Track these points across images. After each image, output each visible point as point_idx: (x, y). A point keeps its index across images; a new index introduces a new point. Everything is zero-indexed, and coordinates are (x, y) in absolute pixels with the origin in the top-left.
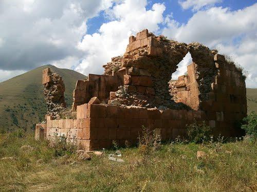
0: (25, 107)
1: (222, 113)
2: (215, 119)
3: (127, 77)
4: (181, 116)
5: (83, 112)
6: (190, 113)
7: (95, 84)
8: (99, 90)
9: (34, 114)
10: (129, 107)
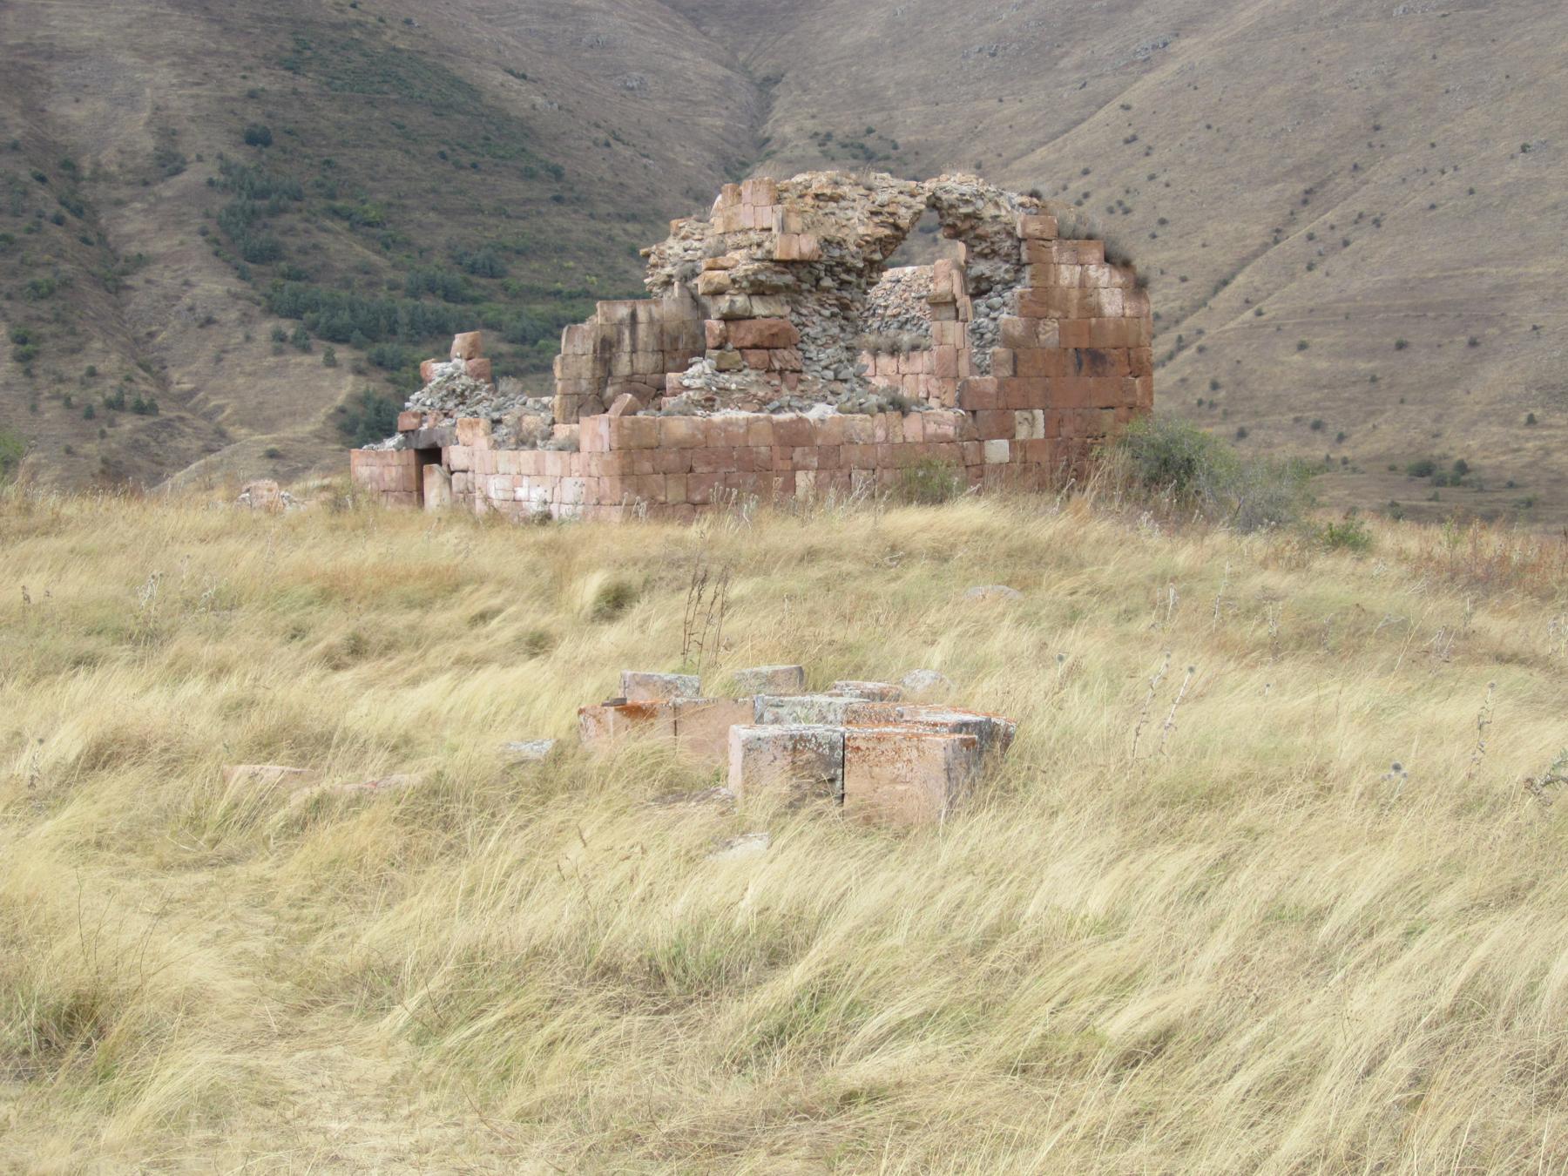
1: (1039, 414)
2: (1008, 432)
4: (880, 434)
7: (620, 333)
8: (634, 351)
10: (717, 417)
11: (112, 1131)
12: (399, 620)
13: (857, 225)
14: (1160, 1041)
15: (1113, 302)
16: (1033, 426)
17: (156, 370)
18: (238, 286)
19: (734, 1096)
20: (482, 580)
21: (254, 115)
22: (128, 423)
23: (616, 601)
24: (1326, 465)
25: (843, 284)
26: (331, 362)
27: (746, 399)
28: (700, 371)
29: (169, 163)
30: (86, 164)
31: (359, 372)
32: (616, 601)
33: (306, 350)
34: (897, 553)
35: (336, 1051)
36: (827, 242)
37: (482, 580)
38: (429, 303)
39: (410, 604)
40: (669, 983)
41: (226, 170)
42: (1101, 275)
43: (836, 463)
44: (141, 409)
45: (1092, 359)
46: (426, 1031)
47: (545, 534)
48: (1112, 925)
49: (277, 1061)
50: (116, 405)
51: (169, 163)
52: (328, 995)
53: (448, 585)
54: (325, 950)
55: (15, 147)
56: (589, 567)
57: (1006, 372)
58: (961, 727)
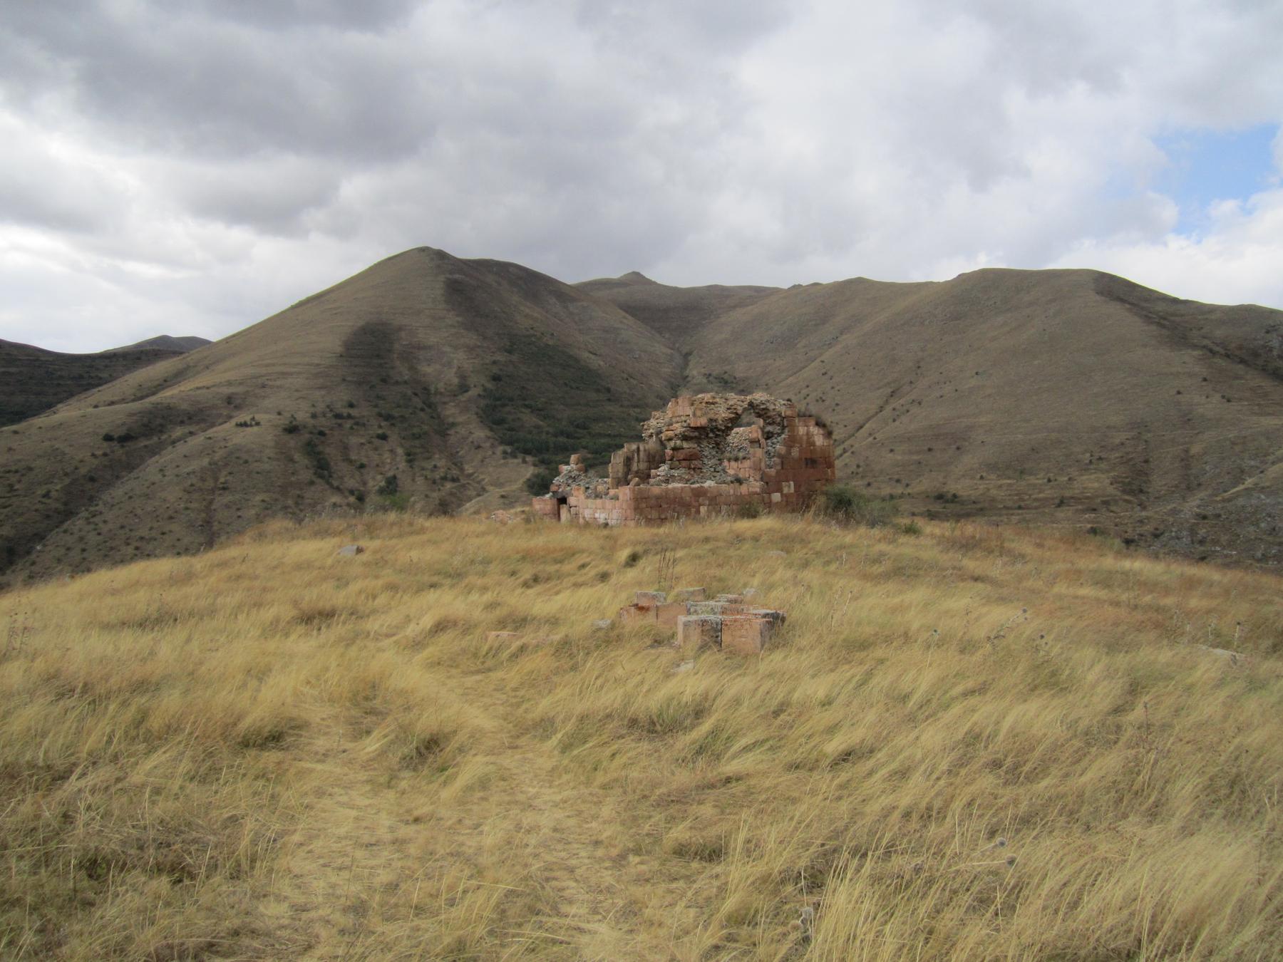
0: (349, 416)
2: (780, 490)
9: (383, 437)
10: (670, 486)
11: (446, 794)
12: (551, 568)
13: (722, 413)
14: (847, 756)
15: (819, 440)
16: (789, 488)
17: (459, 465)
18: (489, 434)
19: (684, 778)
20: (582, 551)
21: (495, 370)
22: (449, 485)
23: (634, 559)
24: (902, 496)
25: (717, 436)
26: (524, 462)
27: (681, 479)
28: (663, 469)
29: (464, 388)
30: (433, 390)
31: (535, 465)
32: (634, 559)
33: (515, 457)
34: (739, 538)
35: (530, 755)
36: (711, 420)
37: (582, 551)
38: (561, 439)
39: (556, 561)
40: (655, 727)
41: (485, 390)
42: (815, 430)
43: (715, 502)
44: (454, 480)
45: (811, 462)
46: (566, 747)
47: (606, 532)
48: (827, 703)
49: (509, 761)
50: (444, 479)
51: (464, 388)
52: (527, 730)
53: (571, 553)
54: (526, 711)
55: (406, 382)
56: (625, 546)
57: (779, 467)
58: (765, 616)
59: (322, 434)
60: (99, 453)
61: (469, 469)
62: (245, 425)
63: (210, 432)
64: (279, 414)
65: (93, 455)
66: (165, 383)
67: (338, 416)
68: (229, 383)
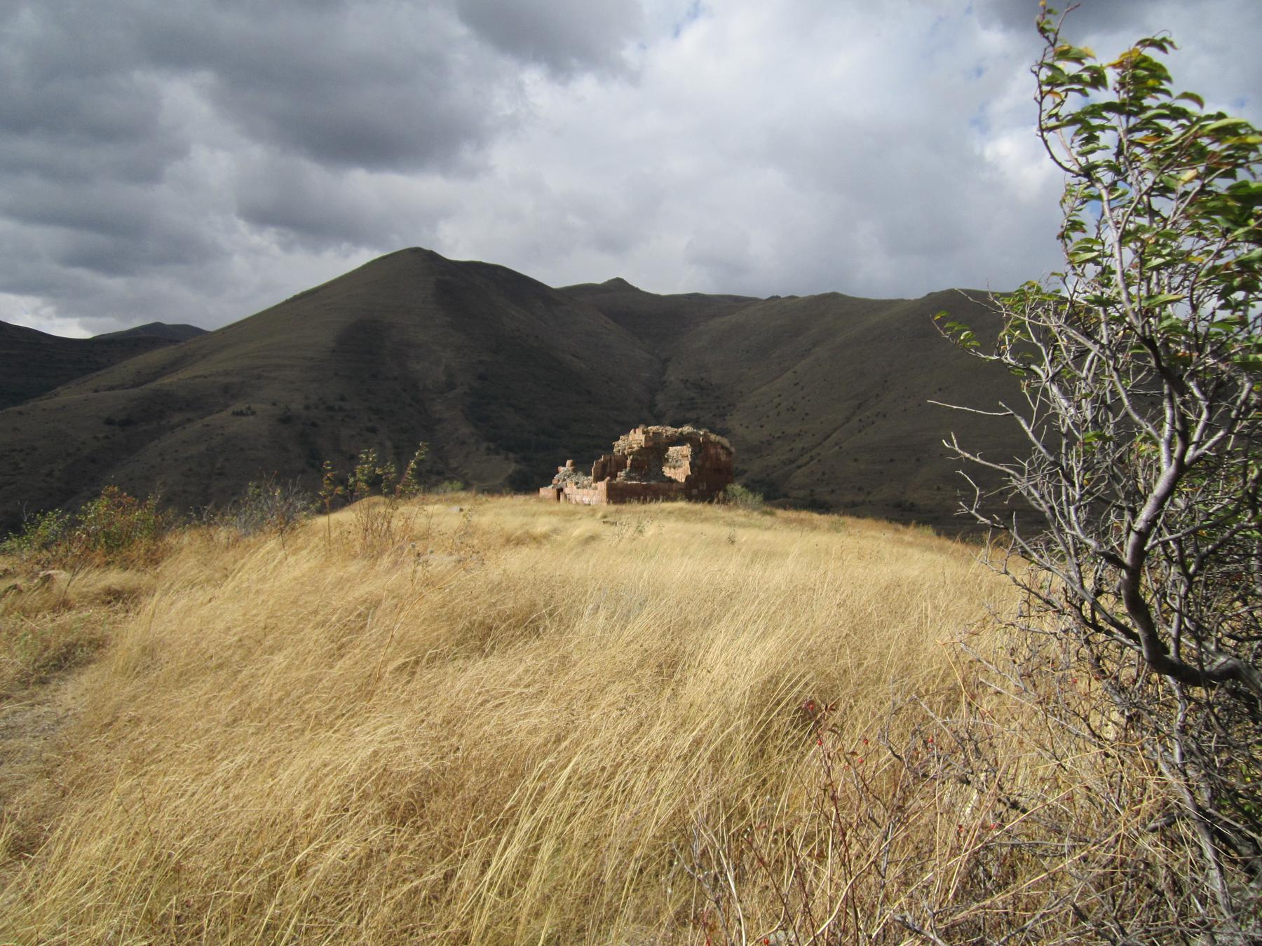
0: (341, 409)
3: (629, 462)
5: (602, 485)
6: (674, 485)
9: (373, 430)
16: (703, 486)
26: (507, 458)
29: (451, 386)
33: (498, 454)
42: (721, 451)
44: (438, 473)
50: (430, 472)
51: (451, 386)
59: (314, 425)
60: (101, 435)
61: (453, 463)
62: (240, 414)
63: (208, 419)
64: (274, 404)
65: (95, 437)
66: (163, 370)
67: (330, 408)
68: (227, 373)
